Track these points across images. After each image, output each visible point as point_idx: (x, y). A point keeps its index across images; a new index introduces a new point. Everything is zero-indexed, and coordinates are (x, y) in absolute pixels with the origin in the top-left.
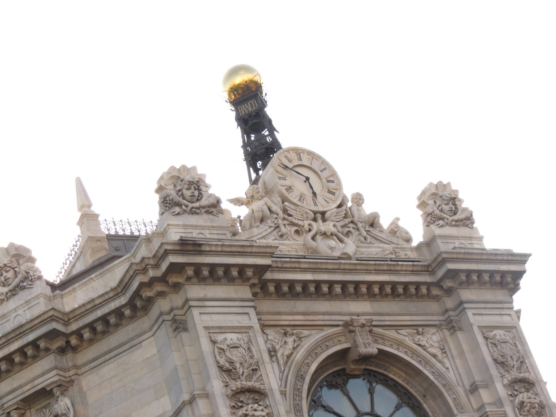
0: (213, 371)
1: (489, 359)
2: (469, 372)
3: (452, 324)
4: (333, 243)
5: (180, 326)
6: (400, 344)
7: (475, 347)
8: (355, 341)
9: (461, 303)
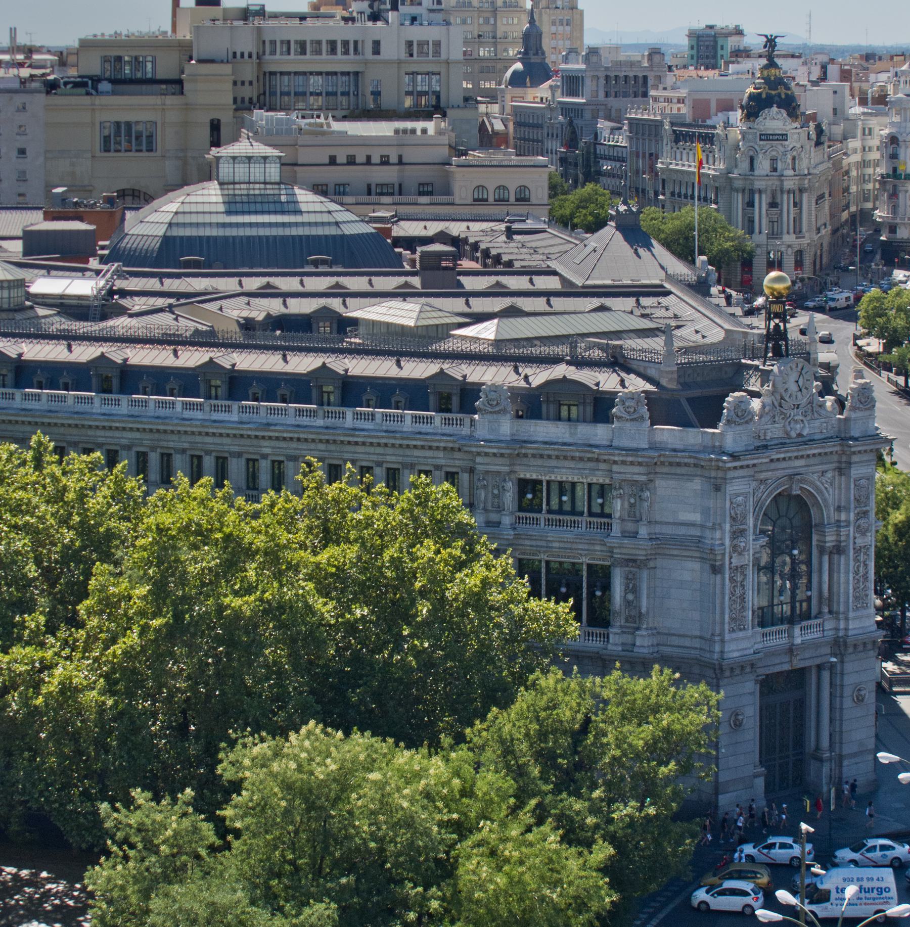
0: (728, 519)
1: (852, 498)
2: (840, 499)
3: (843, 469)
4: (798, 426)
5: (717, 488)
6: (812, 484)
7: (848, 489)
8: (791, 487)
9: (850, 463)
